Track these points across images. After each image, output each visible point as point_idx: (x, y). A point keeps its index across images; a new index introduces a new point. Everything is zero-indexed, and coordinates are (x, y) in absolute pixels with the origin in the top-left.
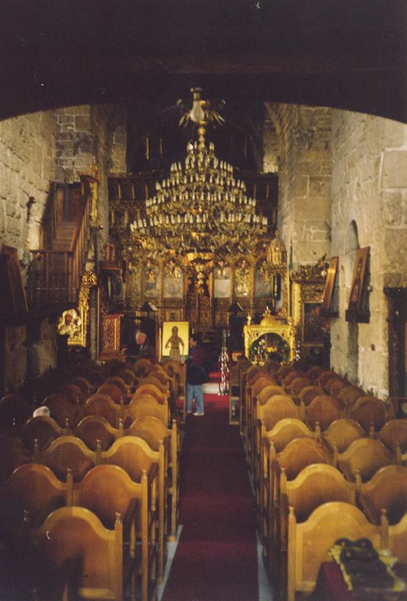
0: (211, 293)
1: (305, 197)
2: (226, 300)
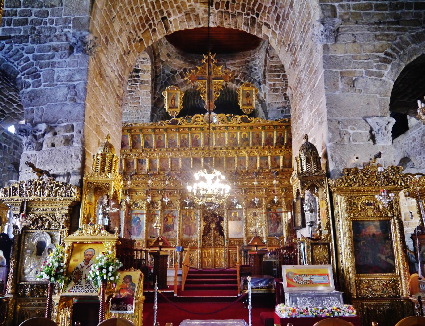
0: (225, 234)
1: (337, 93)
2: (240, 241)
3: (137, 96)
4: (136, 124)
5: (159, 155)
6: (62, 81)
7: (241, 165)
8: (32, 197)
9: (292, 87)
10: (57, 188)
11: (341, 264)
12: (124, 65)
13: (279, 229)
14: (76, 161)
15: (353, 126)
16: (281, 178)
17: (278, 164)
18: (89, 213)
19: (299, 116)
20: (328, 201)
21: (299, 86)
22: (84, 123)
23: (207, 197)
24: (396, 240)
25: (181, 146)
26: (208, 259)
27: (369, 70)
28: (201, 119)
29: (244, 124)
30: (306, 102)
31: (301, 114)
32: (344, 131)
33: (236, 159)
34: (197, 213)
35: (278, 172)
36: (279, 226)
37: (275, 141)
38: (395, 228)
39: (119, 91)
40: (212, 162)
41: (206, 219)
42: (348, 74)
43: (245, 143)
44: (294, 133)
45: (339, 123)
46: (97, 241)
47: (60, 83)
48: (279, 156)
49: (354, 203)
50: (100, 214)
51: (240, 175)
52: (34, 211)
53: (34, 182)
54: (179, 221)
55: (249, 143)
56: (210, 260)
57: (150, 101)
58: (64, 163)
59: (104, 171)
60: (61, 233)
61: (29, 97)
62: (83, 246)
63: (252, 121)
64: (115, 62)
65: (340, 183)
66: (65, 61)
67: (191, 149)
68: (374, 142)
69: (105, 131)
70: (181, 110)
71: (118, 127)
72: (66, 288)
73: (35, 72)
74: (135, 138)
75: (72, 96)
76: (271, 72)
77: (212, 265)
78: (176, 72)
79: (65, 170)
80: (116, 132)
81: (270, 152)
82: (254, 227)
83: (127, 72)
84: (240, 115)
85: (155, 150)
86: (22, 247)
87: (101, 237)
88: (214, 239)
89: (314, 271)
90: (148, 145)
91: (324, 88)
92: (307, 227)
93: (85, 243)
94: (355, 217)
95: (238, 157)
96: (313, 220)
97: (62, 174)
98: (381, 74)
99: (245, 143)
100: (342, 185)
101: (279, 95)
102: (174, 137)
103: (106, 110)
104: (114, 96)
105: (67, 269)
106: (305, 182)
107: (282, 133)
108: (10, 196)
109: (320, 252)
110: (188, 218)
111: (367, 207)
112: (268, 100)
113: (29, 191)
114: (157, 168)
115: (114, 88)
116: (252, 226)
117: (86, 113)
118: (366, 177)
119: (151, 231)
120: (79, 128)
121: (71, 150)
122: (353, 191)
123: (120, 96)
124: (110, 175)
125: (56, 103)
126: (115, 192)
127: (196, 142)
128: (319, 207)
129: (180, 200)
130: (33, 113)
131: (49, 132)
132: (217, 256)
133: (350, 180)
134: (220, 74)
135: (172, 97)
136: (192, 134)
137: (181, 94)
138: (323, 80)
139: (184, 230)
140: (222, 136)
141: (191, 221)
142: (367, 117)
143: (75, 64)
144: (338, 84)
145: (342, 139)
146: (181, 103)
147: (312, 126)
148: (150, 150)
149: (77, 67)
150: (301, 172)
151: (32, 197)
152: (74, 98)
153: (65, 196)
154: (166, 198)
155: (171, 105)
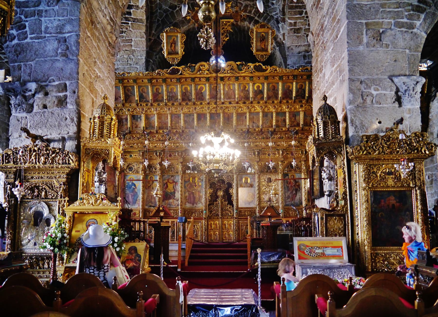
0: (235, 203)
1: (361, 48)
2: (252, 211)
3: (128, 37)
4: (129, 73)
5: (156, 110)
6: (50, 34)
7: (254, 122)
8: (27, 164)
9: (314, 33)
10: (53, 155)
11: (357, 236)
12: (116, 7)
13: (298, 197)
14: (72, 124)
15: (377, 87)
16: (301, 138)
17: (298, 122)
18: (88, 181)
19: (320, 69)
20: (346, 169)
21: (321, 33)
22: (78, 82)
23: (214, 163)
24: (417, 212)
25: (183, 100)
26: (215, 232)
27: (399, 20)
28: (206, 68)
29: (257, 74)
30: (328, 54)
31: (323, 67)
32: (366, 92)
33: (248, 116)
34: (202, 179)
35: (297, 131)
36: (298, 194)
37: (294, 94)
38: (417, 199)
39: (111, 38)
40: (220, 118)
41: (212, 185)
42: (374, 26)
43: (258, 96)
44: (315, 87)
45: (361, 82)
46: (100, 211)
47: (48, 35)
48: (299, 112)
49: (374, 172)
50: (96, 182)
51: (252, 134)
52: (29, 179)
53: (28, 149)
54: (181, 187)
55: (263, 96)
56: (217, 233)
57: (145, 44)
58: (59, 126)
59: (102, 137)
60: (60, 203)
61: (15, 52)
62: (84, 216)
63: (268, 69)
64: (106, 3)
65: (358, 151)
66: (53, 9)
67: (194, 104)
68: (400, 105)
69: (99, 86)
70: (183, 56)
71: (111, 80)
72: (69, 259)
73: (19, 22)
74: (128, 90)
75: (63, 50)
76: (291, 8)
77: (219, 237)
78: (176, 7)
79: (59, 134)
80: (110, 87)
81: (288, 108)
82: (268, 194)
83: (119, 14)
84: (253, 63)
85: (152, 105)
86: (18, 217)
87: (103, 207)
88: (222, 209)
89: (327, 244)
90: (144, 99)
91: (346, 42)
92: (326, 196)
93: (85, 213)
94: (373, 187)
95: (250, 113)
96: (333, 189)
97: (56, 138)
98: (412, 26)
99: (259, 96)
100: (360, 152)
101: (300, 36)
102: (174, 88)
103: (99, 63)
104: (106, 45)
105: (70, 239)
106: (322, 149)
107: (303, 84)
108: (3, 164)
109: (335, 224)
110: (191, 184)
111: (387, 176)
112: (287, 43)
113: (23, 158)
114: (155, 125)
115: (106, 35)
116: (266, 194)
117: (79, 71)
118: (387, 145)
119: (148, 200)
120: (73, 88)
121: (65, 112)
122: (372, 159)
123: (112, 43)
124: (109, 141)
125: (46, 59)
126: (115, 158)
127: (200, 95)
128: (337, 175)
129: (182, 163)
130: (21, 70)
131: (40, 92)
132: (226, 227)
133: (370, 147)
134: (229, 12)
135: (171, 41)
136: (196, 85)
137: (182, 37)
138: (346, 33)
139: (187, 198)
140: (231, 88)
141: (196, 188)
142: (394, 76)
143: (65, 13)
144: (363, 38)
145: (364, 101)
146: (182, 47)
147: (333, 83)
148: (147, 105)
149: (67, 16)
150: (317, 137)
151: (27, 165)
152: (65, 53)
153: (63, 164)
154: (166, 161)
155: (170, 51)
